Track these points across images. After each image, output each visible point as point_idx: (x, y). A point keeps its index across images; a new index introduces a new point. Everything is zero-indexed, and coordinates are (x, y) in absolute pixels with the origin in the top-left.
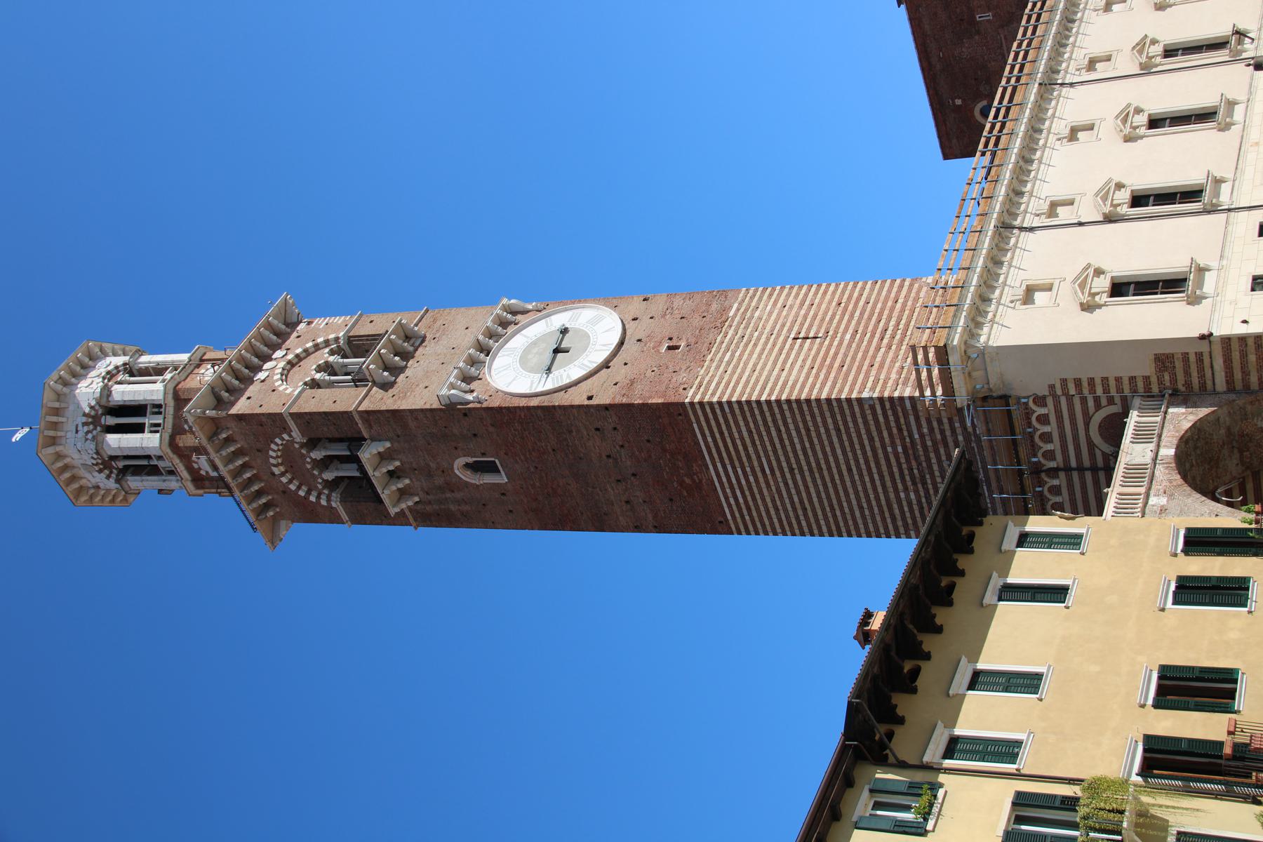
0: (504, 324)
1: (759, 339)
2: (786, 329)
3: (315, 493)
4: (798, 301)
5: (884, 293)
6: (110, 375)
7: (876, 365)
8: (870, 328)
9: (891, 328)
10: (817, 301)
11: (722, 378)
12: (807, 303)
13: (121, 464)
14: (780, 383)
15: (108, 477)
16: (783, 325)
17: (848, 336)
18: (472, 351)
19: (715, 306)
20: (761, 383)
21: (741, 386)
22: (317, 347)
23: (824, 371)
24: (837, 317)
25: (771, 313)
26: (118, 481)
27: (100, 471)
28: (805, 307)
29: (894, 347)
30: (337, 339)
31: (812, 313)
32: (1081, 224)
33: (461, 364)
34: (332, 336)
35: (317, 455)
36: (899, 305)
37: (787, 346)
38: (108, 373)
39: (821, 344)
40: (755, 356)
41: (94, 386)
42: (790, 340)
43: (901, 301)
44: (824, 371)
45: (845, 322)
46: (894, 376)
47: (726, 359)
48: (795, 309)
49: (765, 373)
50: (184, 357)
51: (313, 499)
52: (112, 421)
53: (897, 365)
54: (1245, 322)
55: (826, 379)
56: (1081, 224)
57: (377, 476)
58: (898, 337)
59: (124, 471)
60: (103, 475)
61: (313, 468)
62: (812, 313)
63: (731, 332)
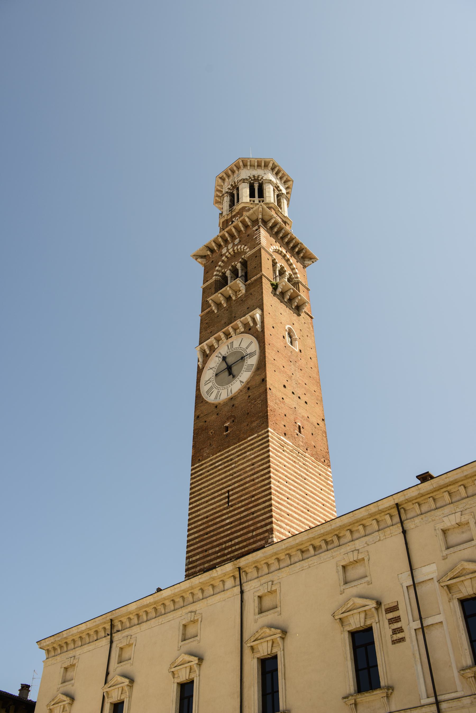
3: (220, 269)
6: (277, 187)
13: (235, 192)
15: (229, 189)
22: (293, 269)
26: (227, 192)
27: (232, 185)
30: (297, 278)
34: (298, 276)
35: (239, 266)
50: (286, 214)
51: (217, 268)
52: (256, 186)
57: (227, 290)
59: (232, 195)
60: (230, 186)
61: (232, 266)
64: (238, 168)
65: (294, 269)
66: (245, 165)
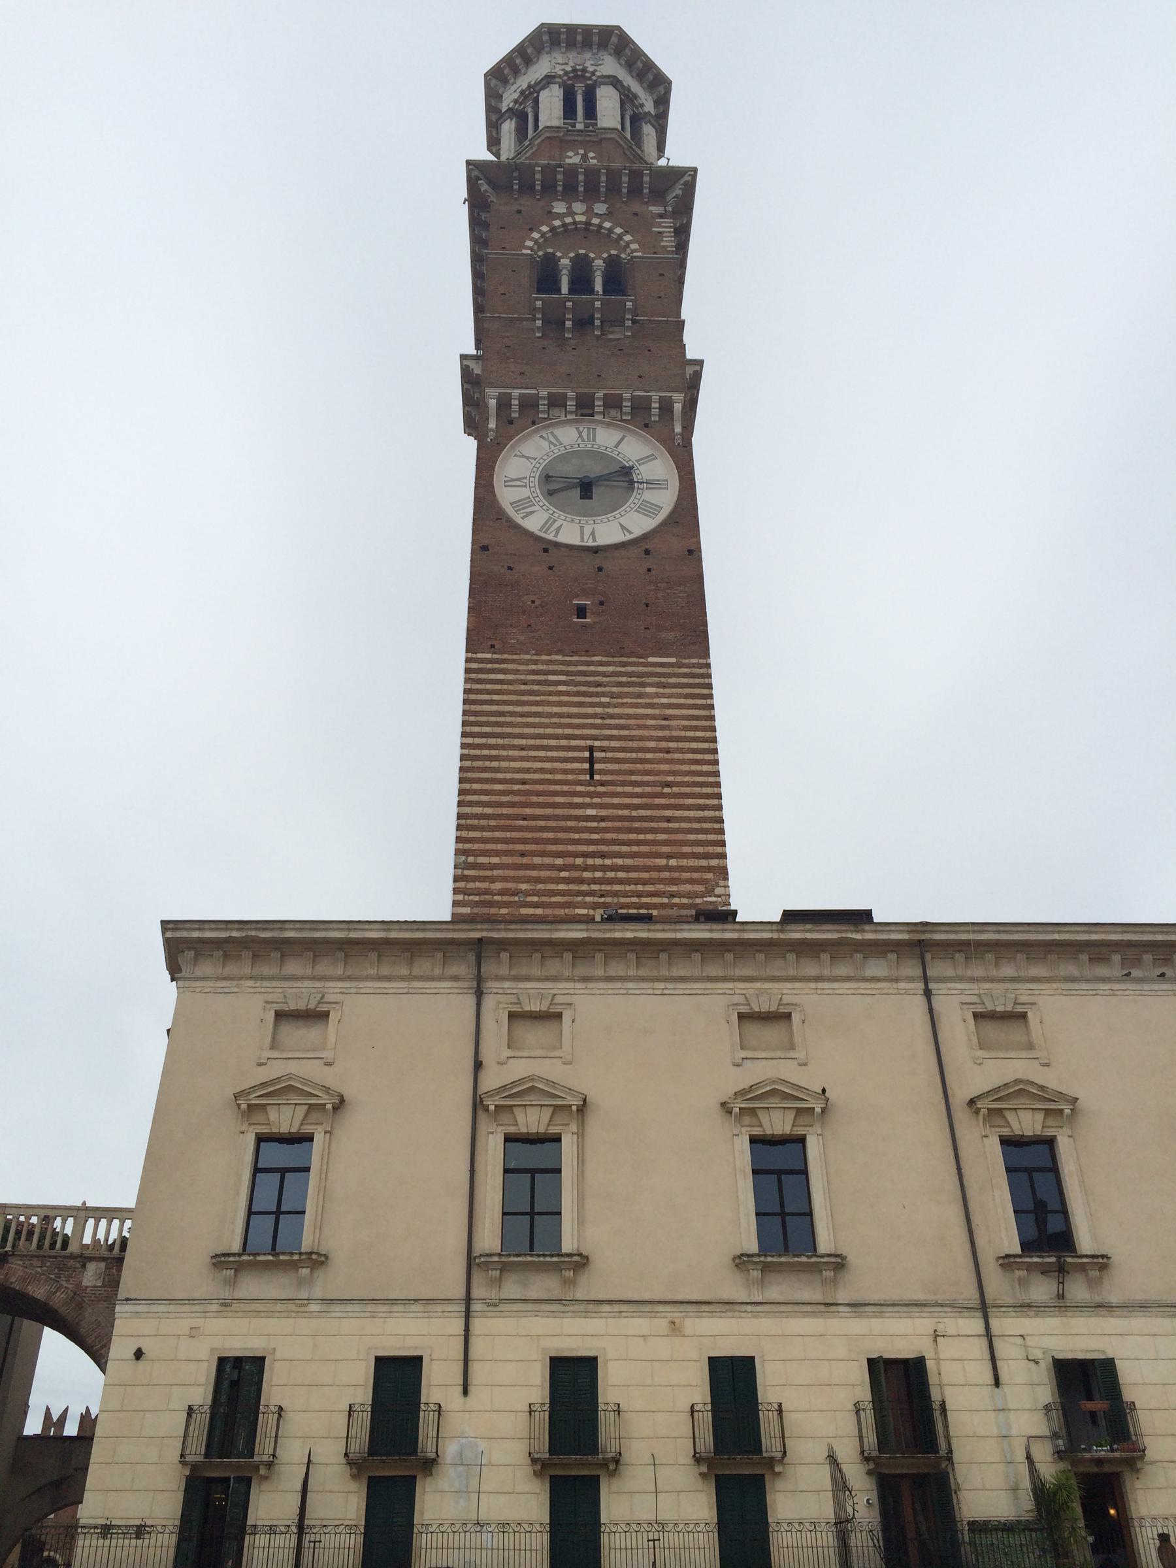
0: (640, 408)
1: (593, 705)
2: (615, 732)
4: (675, 733)
5: (692, 837)
6: (579, 74)
7: (525, 860)
8: (608, 836)
9: (608, 862)
10: (677, 756)
11: (510, 682)
12: (672, 745)
14: (494, 753)
16: (622, 727)
17: (591, 812)
18: (571, 394)
19: (670, 635)
20: (498, 730)
21: (494, 708)
23: (516, 799)
24: (638, 790)
25: (651, 706)
28: (664, 745)
29: (564, 874)
31: (649, 756)
32: (478, 1065)
33: (544, 393)
34: (634, 246)
36: (662, 862)
37: (574, 743)
38: (584, 70)
39: (580, 783)
40: (555, 710)
41: (559, 67)
42: (589, 743)
43: (673, 862)
44: (516, 799)
45: (627, 801)
46: (498, 886)
47: (551, 678)
48: (660, 733)
49: (517, 730)
53: (524, 887)
54: (139, 1354)
55: (500, 805)
56: (478, 1065)
58: (587, 875)
62: (649, 756)
63: (610, 669)
64: (500, 97)
65: (620, 237)
66: (505, 81)
